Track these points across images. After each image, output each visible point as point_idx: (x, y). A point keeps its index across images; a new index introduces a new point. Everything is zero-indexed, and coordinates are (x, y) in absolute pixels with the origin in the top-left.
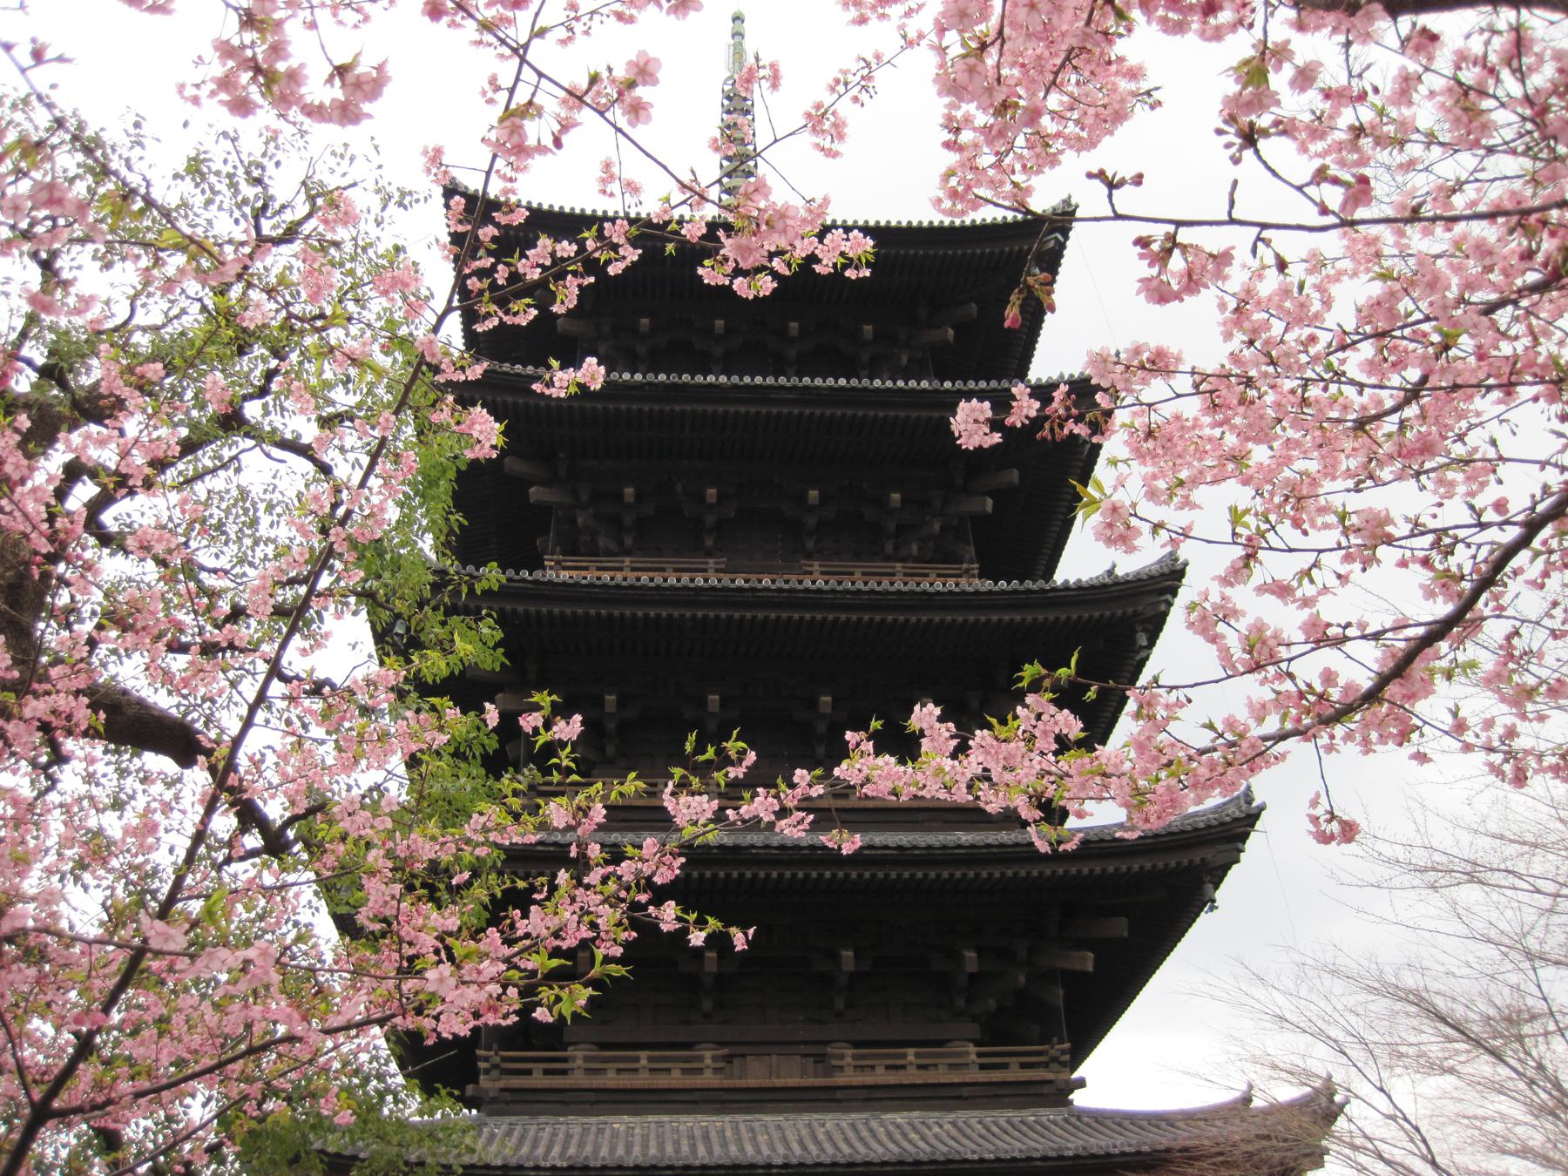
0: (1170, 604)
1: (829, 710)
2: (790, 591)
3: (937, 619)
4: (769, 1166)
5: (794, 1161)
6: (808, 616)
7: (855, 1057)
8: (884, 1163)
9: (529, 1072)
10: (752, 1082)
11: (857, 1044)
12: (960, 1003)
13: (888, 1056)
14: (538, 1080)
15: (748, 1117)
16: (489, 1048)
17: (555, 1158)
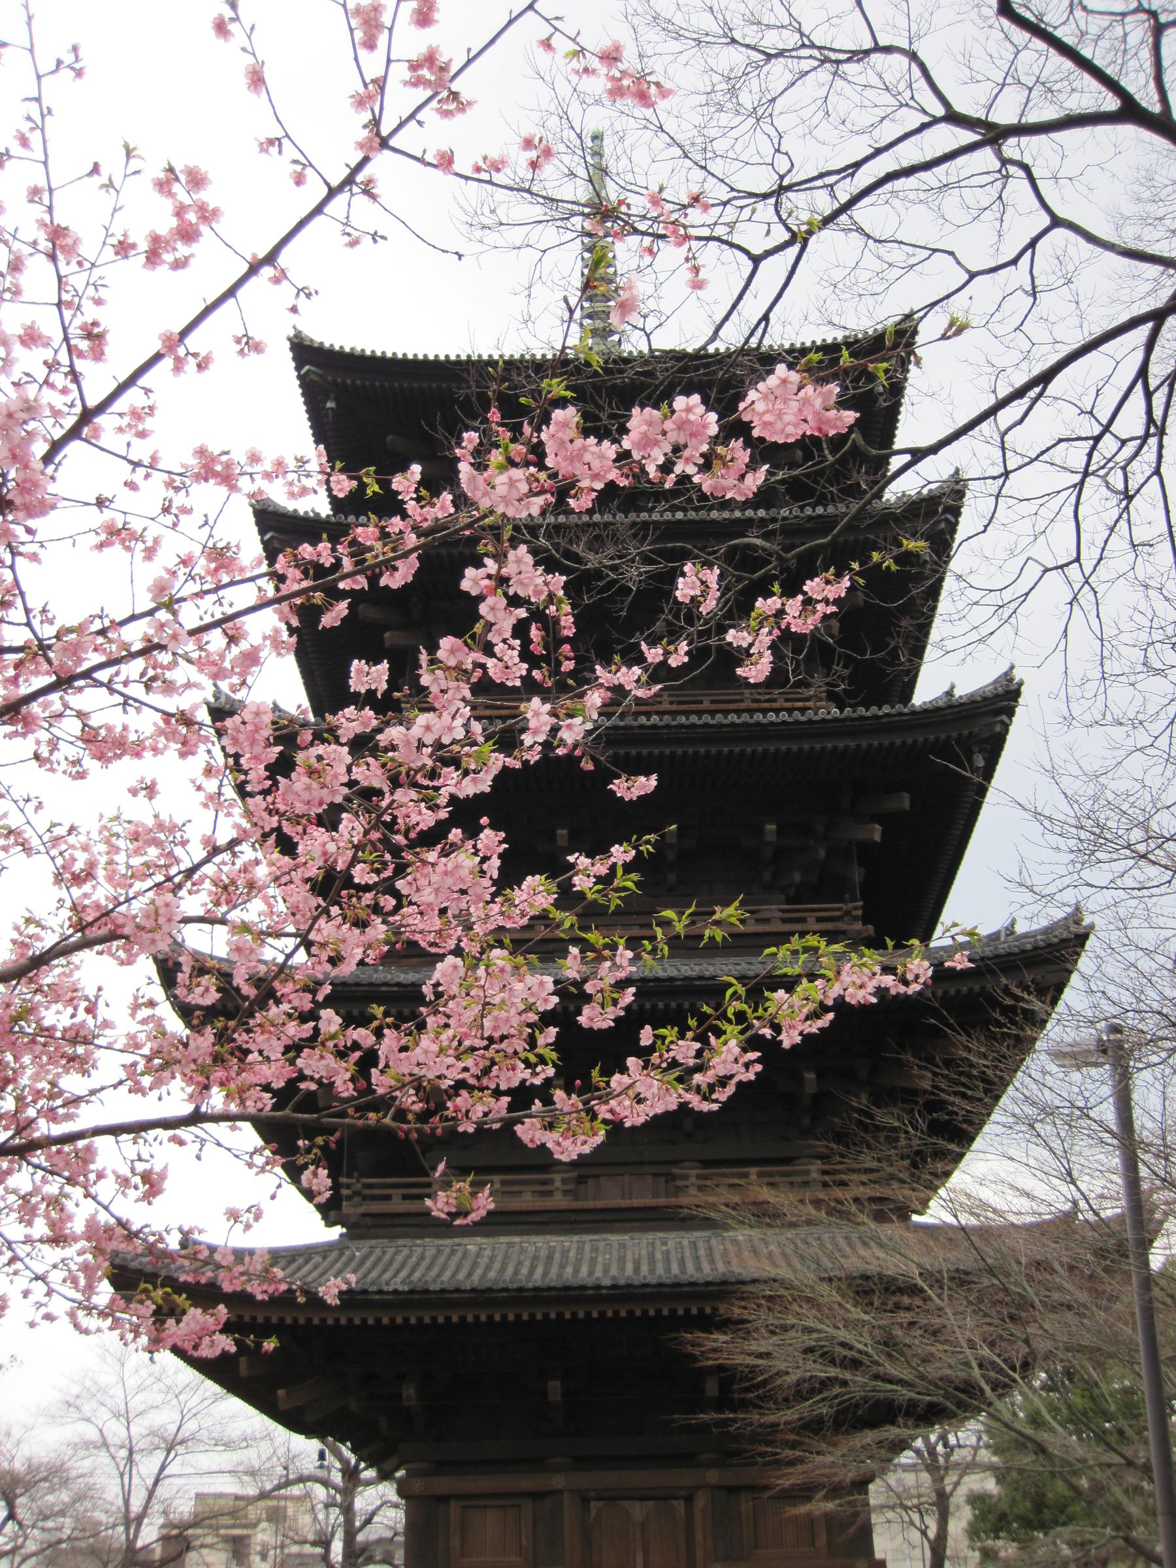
0: (1006, 728)
1: (674, 840)
2: (625, 728)
3: (772, 749)
4: (598, 1287)
5: (622, 1282)
6: (645, 752)
7: (698, 1177)
8: (708, 1284)
9: (388, 1198)
10: (599, 1204)
11: (706, 1163)
12: (806, 1121)
13: (733, 1175)
14: (398, 1205)
15: (595, 1237)
16: (349, 1176)
17: (398, 1284)
